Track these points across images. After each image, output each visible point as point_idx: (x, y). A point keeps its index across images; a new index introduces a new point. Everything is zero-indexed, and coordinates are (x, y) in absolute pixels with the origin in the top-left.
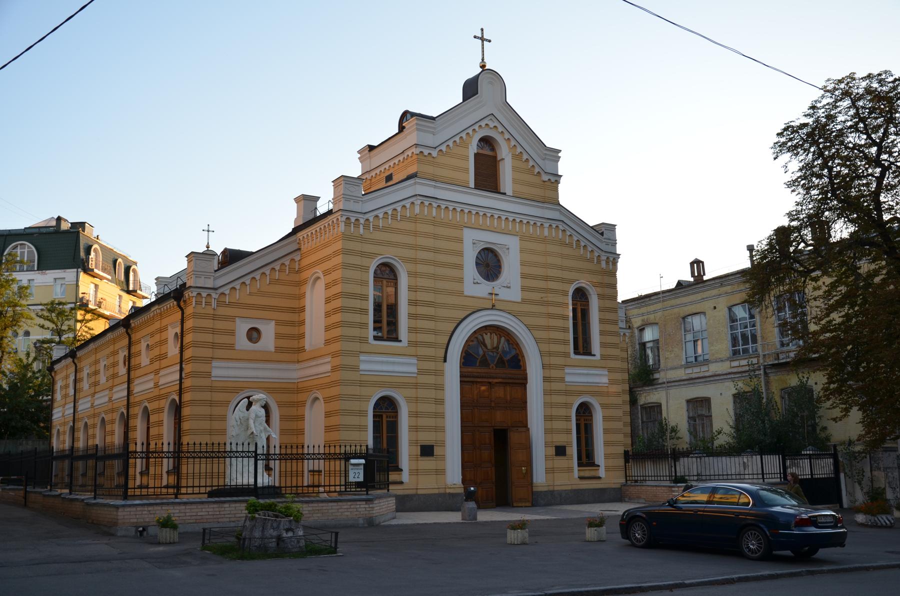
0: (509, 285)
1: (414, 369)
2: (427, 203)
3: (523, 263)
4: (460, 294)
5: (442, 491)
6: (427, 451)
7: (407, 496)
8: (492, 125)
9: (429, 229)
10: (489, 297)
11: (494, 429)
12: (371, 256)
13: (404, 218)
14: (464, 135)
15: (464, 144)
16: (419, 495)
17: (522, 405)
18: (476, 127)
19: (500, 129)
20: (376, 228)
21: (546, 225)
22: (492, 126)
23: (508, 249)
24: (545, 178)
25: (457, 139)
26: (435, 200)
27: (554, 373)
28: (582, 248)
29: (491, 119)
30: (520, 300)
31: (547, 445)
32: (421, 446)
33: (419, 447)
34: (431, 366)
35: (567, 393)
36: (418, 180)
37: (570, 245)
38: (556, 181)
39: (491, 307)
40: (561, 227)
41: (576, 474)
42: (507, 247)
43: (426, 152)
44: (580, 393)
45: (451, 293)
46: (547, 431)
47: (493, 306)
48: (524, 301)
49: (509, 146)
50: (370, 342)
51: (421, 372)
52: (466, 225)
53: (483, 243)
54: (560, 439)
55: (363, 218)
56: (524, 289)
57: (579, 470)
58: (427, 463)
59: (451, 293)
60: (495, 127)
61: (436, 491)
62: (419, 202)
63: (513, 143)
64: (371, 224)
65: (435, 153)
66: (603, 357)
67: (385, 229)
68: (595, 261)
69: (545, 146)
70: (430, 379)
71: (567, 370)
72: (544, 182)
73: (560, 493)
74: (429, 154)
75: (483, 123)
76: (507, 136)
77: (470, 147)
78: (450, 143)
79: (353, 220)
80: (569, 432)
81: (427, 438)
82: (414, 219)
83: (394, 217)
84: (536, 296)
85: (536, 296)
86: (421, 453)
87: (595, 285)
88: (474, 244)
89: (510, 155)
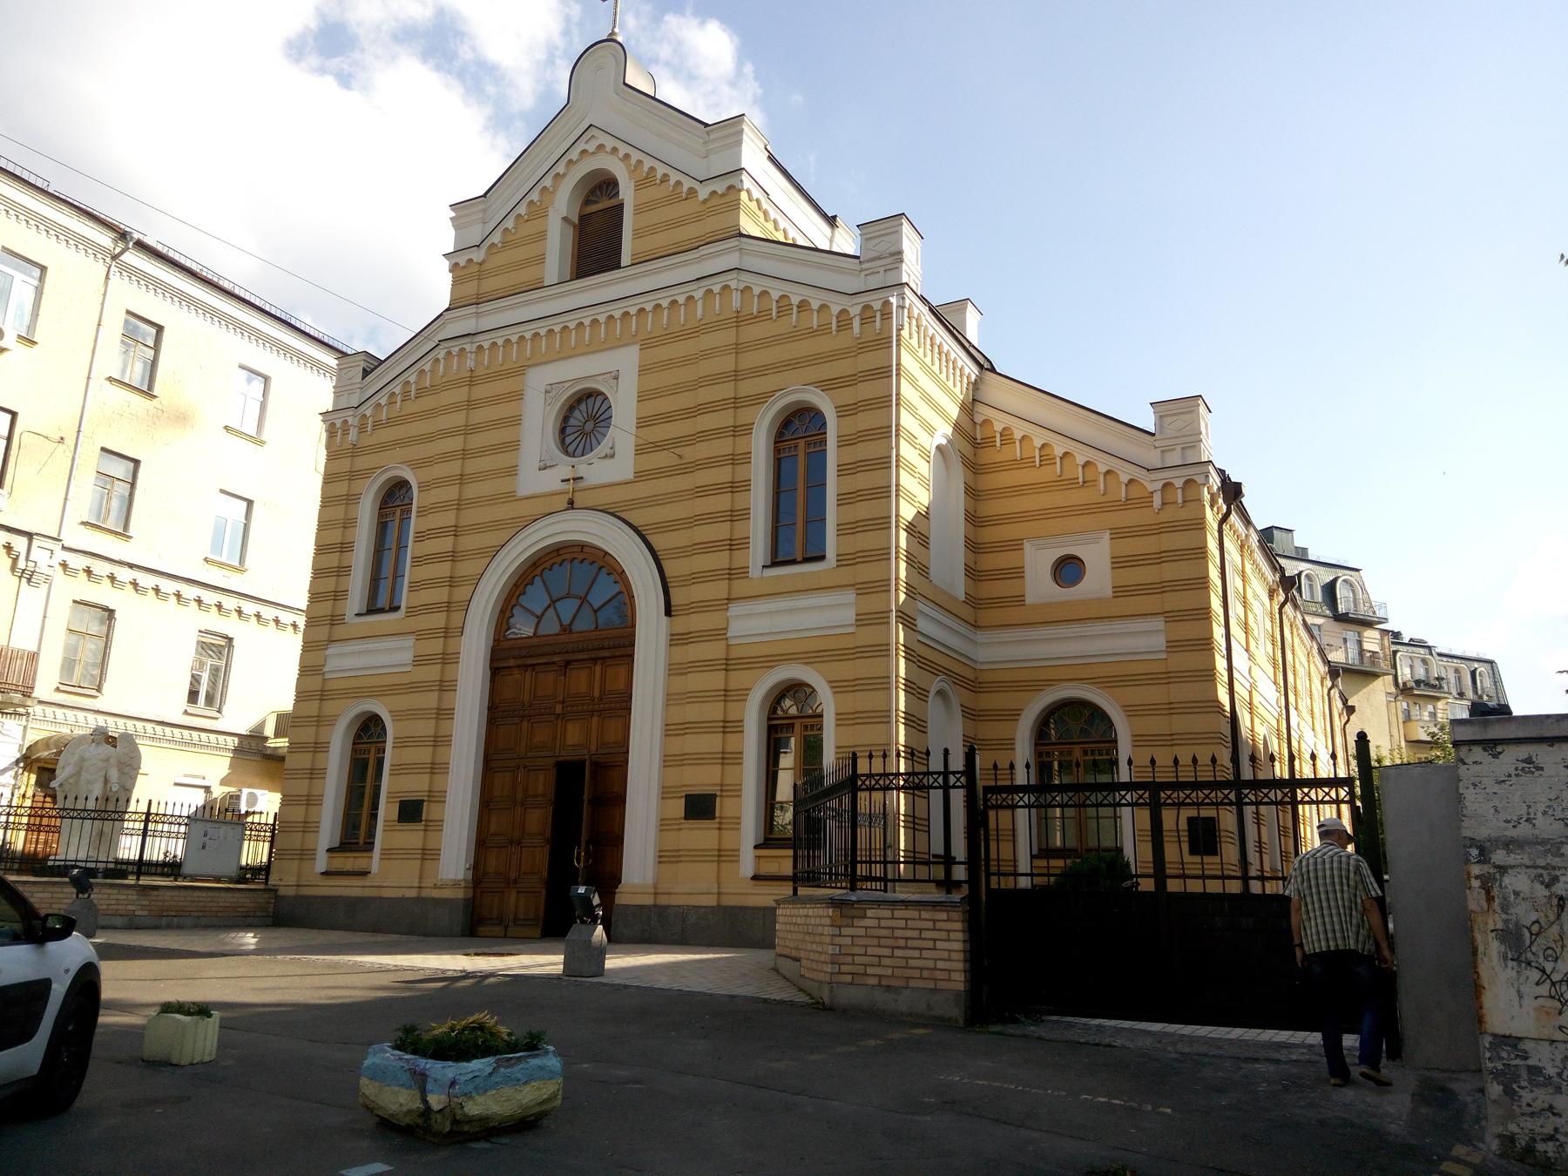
0: (609, 452)
1: (408, 657)
2: (455, 350)
3: (642, 397)
4: (510, 497)
5: (426, 893)
6: (410, 811)
7: (361, 900)
8: (591, 147)
9: (460, 394)
10: (564, 486)
11: (558, 762)
12: (365, 474)
13: (421, 393)
14: (535, 196)
15: (538, 212)
16: (381, 898)
17: (620, 705)
18: (560, 168)
19: (610, 143)
20: (377, 425)
21: (698, 295)
22: (591, 147)
23: (616, 378)
24: (703, 193)
25: (522, 209)
26: (468, 339)
27: (697, 622)
28: (795, 308)
29: (593, 136)
30: (630, 476)
31: (666, 793)
32: (401, 801)
33: (397, 806)
34: (435, 646)
35: (728, 665)
36: (448, 315)
37: (763, 316)
38: (731, 188)
39: (566, 505)
40: (733, 285)
41: (747, 863)
42: (613, 374)
43: (462, 261)
44: (770, 661)
45: (494, 499)
46: (669, 761)
47: (571, 504)
48: (641, 476)
49: (628, 167)
50: (346, 621)
51: (419, 661)
52: (531, 362)
53: (567, 385)
54: (702, 779)
55: (354, 416)
56: (640, 450)
57: (758, 857)
58: (411, 836)
59: (494, 499)
60: (601, 147)
61: (413, 893)
62: (441, 356)
63: (636, 156)
64: (370, 421)
65: (478, 256)
66: (844, 560)
67: (391, 422)
68: (834, 328)
69: (706, 125)
70: (432, 673)
71: (735, 609)
72: (705, 201)
73: (683, 912)
74: (470, 261)
75: (574, 155)
76: (623, 149)
77: (551, 212)
78: (510, 223)
79: (338, 423)
80: (729, 759)
81: (414, 786)
82: (434, 389)
83: (406, 395)
84: (664, 459)
85: (664, 459)
86: (399, 817)
87: (827, 385)
88: (546, 392)
89: (633, 184)
